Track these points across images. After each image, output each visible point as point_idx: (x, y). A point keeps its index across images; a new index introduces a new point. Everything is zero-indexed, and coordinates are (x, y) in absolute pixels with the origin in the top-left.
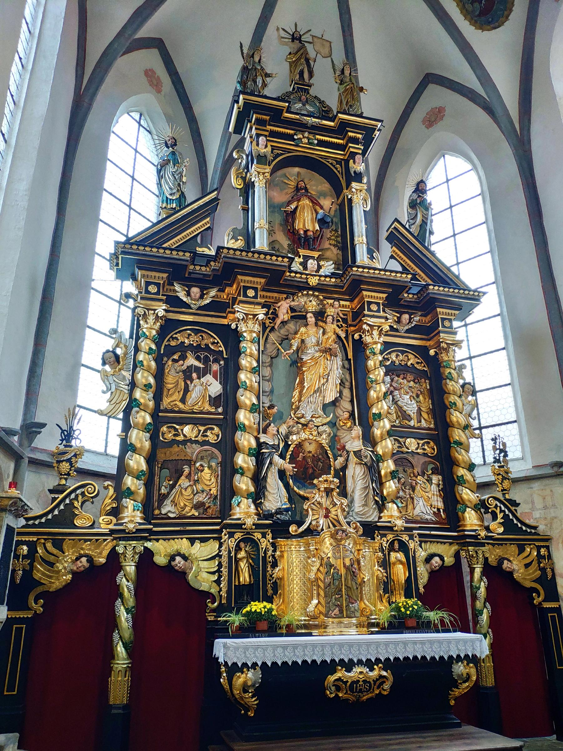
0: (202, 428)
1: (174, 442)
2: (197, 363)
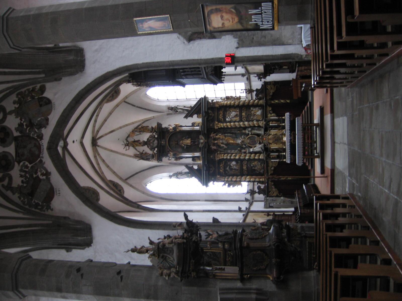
0: (244, 165)
2: (228, 167)
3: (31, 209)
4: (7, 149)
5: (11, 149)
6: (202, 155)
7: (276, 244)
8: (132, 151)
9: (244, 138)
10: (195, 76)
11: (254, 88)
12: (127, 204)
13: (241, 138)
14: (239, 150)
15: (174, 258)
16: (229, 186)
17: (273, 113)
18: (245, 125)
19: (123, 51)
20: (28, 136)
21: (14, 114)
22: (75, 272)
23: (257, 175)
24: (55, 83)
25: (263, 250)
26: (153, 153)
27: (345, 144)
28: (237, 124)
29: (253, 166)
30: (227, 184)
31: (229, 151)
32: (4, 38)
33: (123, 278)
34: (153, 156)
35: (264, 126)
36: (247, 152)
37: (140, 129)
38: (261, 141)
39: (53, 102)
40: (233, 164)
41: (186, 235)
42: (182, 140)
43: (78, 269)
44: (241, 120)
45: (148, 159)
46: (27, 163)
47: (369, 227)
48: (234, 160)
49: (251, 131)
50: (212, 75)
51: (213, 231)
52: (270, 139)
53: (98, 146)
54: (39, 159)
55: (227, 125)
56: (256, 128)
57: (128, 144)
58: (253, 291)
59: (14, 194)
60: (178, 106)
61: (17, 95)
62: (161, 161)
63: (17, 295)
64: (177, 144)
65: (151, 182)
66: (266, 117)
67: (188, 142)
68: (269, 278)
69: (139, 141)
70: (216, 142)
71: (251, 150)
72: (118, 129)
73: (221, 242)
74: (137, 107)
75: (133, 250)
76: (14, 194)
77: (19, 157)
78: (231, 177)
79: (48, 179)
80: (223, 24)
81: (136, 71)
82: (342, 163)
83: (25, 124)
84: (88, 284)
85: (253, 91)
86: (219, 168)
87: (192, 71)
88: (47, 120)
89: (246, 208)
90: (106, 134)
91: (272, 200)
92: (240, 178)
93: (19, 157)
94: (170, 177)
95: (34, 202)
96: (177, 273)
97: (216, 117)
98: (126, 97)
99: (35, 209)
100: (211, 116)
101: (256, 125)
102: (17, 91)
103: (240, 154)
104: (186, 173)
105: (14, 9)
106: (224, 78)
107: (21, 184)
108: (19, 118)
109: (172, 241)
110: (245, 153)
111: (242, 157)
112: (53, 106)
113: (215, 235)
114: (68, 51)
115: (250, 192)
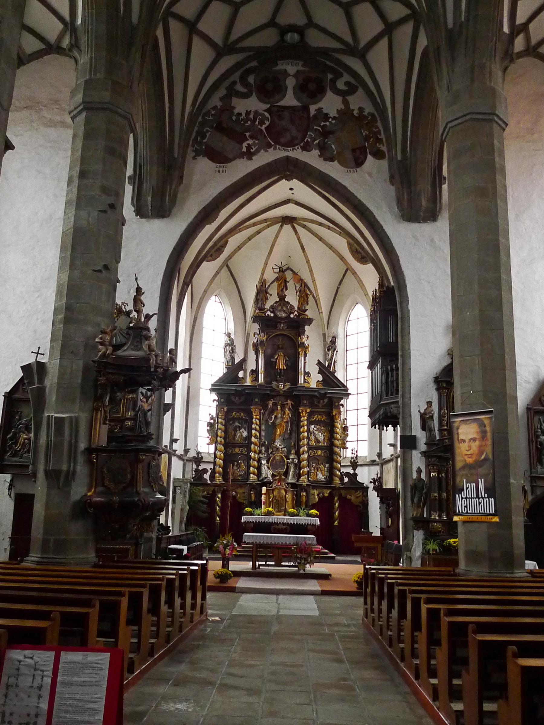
0: (241, 449)
1: (232, 454)
2: (238, 425)
3: (197, 124)
4: (290, 92)
5: (290, 100)
6: (261, 385)
7: (141, 504)
8: (270, 276)
9: (283, 452)
10: (384, 387)
11: (358, 471)
12: (191, 267)
13: (282, 446)
14: (265, 442)
15: (127, 352)
16: (210, 424)
17: (319, 499)
18: (303, 454)
19: (429, 282)
20: (308, 128)
21: (343, 108)
22: (109, 202)
23: (225, 468)
24: (387, 175)
25: (133, 483)
26: (266, 310)
27: (278, 611)
28: (306, 441)
29: (238, 464)
30: (212, 421)
31: (263, 427)
32: (461, 114)
33: (99, 274)
34: (261, 309)
35: (300, 482)
36: (261, 456)
37: (304, 291)
38: (277, 478)
39: (358, 169)
40: (243, 432)
41: (160, 370)
42: (284, 356)
43: (115, 207)
44: (310, 448)
45: (257, 300)
46: (267, 123)
47: (169, 643)
48: (250, 435)
49: (293, 462)
50: (385, 413)
51: (151, 404)
52: (279, 492)
53: (282, 226)
54: (273, 144)
55: (303, 426)
56: (297, 471)
57: (282, 270)
58: (72, 466)
59: (221, 99)
60: (337, 352)
61: (372, 115)
62: (254, 322)
63: (75, 109)
64: (278, 348)
65: (221, 303)
66: (314, 488)
67: (282, 365)
68: (89, 491)
69: (287, 289)
70: (279, 407)
71: (264, 462)
72: (306, 257)
73: (136, 415)
74: (338, 288)
75: (139, 291)
76: (221, 99)
77: (277, 112)
78: (223, 427)
79: (242, 155)
80: (464, 441)
81: (398, 300)
82: (250, 604)
83: (328, 123)
84: (90, 219)
85: (355, 471)
86: (239, 411)
87: (392, 382)
88: (332, 160)
89: (177, 450)
90: (299, 239)
91: (186, 491)
92: (221, 441)
93: (277, 112)
94: (229, 335)
95: (208, 131)
96: (104, 355)
97: (317, 410)
98: (354, 273)
99: (197, 132)
100: (319, 402)
101: (301, 471)
102: (378, 113)
103: (258, 445)
104: (233, 359)
105: (504, 130)
106: (379, 429)
107: (236, 111)
108: (337, 116)
109: (153, 351)
110: (260, 452)
111: (254, 448)
112: (352, 170)
113: (146, 407)
114: (435, 198)
115: (198, 456)
